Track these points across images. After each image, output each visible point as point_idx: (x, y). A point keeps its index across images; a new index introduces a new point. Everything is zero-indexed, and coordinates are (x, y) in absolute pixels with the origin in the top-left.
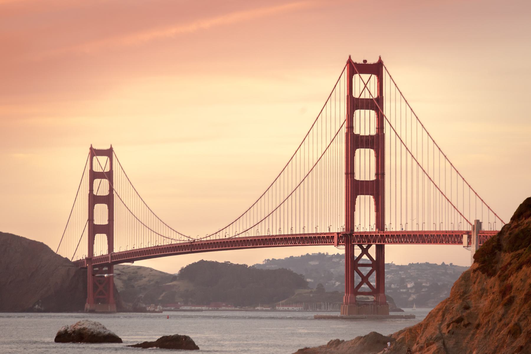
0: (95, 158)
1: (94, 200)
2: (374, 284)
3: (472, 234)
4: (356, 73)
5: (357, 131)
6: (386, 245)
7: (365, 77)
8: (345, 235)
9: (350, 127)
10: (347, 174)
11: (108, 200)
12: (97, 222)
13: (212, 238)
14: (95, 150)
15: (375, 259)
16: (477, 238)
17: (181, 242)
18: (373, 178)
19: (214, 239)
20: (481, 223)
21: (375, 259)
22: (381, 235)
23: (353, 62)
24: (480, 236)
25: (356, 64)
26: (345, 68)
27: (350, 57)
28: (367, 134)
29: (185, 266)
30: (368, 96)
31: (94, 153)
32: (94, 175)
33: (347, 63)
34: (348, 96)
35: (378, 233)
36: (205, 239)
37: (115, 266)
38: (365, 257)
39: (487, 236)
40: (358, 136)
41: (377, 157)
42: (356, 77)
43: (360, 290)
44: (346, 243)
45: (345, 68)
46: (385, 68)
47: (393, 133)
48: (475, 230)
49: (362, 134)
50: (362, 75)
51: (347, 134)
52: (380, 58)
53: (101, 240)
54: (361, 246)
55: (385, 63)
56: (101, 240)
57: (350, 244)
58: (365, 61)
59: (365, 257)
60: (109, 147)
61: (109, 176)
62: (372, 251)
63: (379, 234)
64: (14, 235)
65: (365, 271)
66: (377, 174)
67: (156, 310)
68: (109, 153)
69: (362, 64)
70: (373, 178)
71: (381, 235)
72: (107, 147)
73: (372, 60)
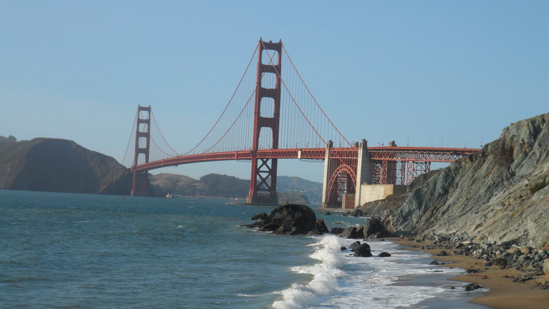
0: (140, 111)
1: (139, 135)
2: (270, 185)
3: (326, 150)
4: (264, 49)
5: (263, 86)
6: (278, 160)
7: (272, 53)
8: (252, 152)
9: (259, 83)
10: (255, 113)
11: (147, 135)
12: (140, 147)
13: (188, 155)
14: (141, 107)
15: (270, 167)
16: (329, 152)
17: (174, 157)
18: (272, 116)
19: (189, 155)
20: (332, 143)
21: (271, 168)
22: (272, 152)
23: (263, 42)
24: (331, 151)
25: (264, 43)
26: (258, 46)
27: (261, 38)
28: (271, 88)
29: (203, 176)
30: (272, 65)
31: (141, 109)
32: (140, 121)
33: (259, 42)
34: (258, 63)
35: (271, 150)
36: (184, 155)
37: (150, 172)
38: (264, 166)
39: (335, 151)
40: (264, 89)
41: (276, 103)
42: (264, 51)
43: (260, 188)
44: (253, 157)
45: (258, 46)
46: (283, 46)
47: (285, 89)
48: (328, 147)
49: (265, 88)
50: (268, 51)
51: (257, 87)
52: (280, 40)
53: (142, 157)
54: (262, 159)
55: (284, 44)
56: (142, 157)
57: (255, 158)
58: (271, 42)
59: (264, 166)
60: (148, 106)
61: (148, 122)
62: (269, 163)
63: (271, 151)
64: (103, 155)
65: (264, 175)
66: (275, 114)
67: (170, 197)
68: (148, 109)
69: (268, 43)
70: (273, 116)
71: (272, 152)
72: (147, 106)
73: (275, 41)
